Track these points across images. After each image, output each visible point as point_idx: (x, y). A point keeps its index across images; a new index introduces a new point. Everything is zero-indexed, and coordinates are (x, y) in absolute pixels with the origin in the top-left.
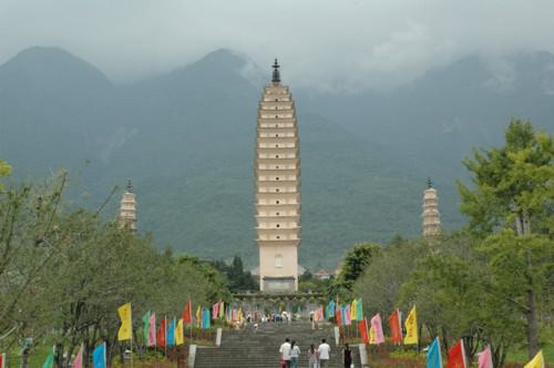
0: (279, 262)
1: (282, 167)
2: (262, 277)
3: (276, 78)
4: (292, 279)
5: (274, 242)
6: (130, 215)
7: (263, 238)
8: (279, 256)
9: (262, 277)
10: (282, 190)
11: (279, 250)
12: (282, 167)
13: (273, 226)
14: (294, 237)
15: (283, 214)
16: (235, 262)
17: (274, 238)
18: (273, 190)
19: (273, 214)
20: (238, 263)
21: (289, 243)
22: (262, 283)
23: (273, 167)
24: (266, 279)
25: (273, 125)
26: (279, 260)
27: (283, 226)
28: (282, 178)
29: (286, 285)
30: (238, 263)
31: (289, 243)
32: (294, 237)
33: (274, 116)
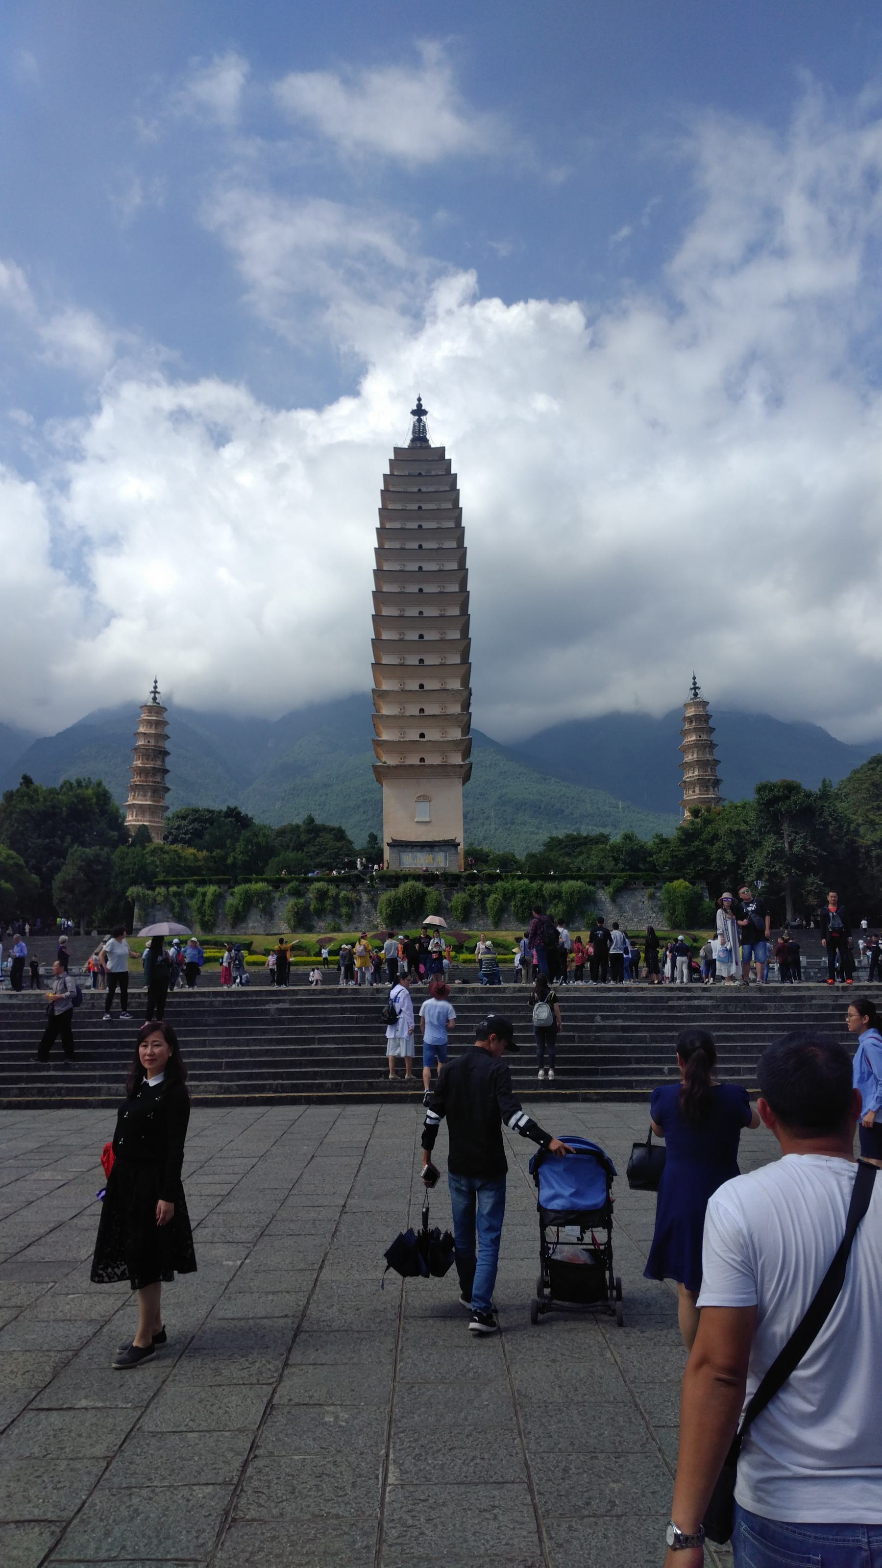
0: (423, 812)
1: (431, 612)
2: (387, 839)
3: (420, 436)
4: (452, 844)
5: (412, 765)
8: (425, 798)
9: (387, 839)
10: (430, 660)
12: (431, 612)
13: (413, 735)
14: (457, 759)
15: (432, 709)
17: (413, 760)
18: (413, 660)
21: (443, 771)
23: (412, 612)
25: (414, 525)
27: (433, 735)
28: (431, 635)
29: (438, 862)
32: (457, 759)
33: (415, 507)
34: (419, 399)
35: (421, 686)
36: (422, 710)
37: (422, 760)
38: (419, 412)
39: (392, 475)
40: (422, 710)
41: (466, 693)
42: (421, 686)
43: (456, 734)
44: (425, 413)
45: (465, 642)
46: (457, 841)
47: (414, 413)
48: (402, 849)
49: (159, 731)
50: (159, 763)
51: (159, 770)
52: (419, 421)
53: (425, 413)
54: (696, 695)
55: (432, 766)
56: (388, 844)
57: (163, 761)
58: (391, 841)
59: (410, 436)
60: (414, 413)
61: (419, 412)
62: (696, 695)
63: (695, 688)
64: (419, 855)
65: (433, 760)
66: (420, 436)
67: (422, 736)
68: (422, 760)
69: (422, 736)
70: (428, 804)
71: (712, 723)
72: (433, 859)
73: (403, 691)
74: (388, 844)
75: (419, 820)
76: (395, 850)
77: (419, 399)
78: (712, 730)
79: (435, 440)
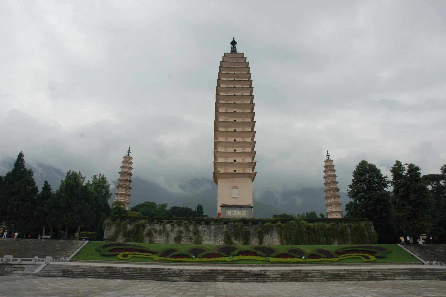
0: (235, 193)
2: (220, 204)
3: (234, 50)
4: (249, 207)
5: (231, 173)
6: (127, 170)
7: (222, 171)
8: (236, 187)
9: (220, 204)
10: (238, 130)
11: (236, 182)
13: (231, 160)
14: (249, 171)
15: (238, 150)
16: (197, 208)
17: (231, 171)
19: (231, 150)
20: (200, 208)
21: (244, 175)
22: (219, 210)
24: (223, 206)
25: (233, 79)
26: (235, 191)
27: (239, 160)
29: (243, 214)
30: (200, 208)
31: (244, 175)
34: (234, 39)
35: (235, 140)
36: (235, 150)
37: (235, 171)
38: (234, 43)
39: (223, 61)
40: (235, 150)
41: (253, 144)
42: (235, 140)
43: (249, 160)
44: (236, 43)
45: (253, 124)
46: (252, 205)
47: (232, 43)
48: (227, 208)
49: (129, 166)
50: (128, 178)
51: (128, 181)
52: (234, 46)
53: (236, 43)
54: (328, 158)
55: (240, 174)
56: (221, 206)
57: (130, 177)
58: (222, 205)
59: (230, 51)
60: (232, 43)
61: (234, 43)
62: (328, 158)
63: (328, 155)
64: (234, 211)
65: (239, 171)
66: (234, 50)
67: (235, 161)
68: (235, 171)
69: (235, 161)
70: (237, 190)
71: (335, 168)
72: (241, 213)
73: (227, 142)
74: (221, 206)
75: (234, 196)
76: (223, 208)
77: (234, 39)
78: (335, 171)
79: (239, 51)
